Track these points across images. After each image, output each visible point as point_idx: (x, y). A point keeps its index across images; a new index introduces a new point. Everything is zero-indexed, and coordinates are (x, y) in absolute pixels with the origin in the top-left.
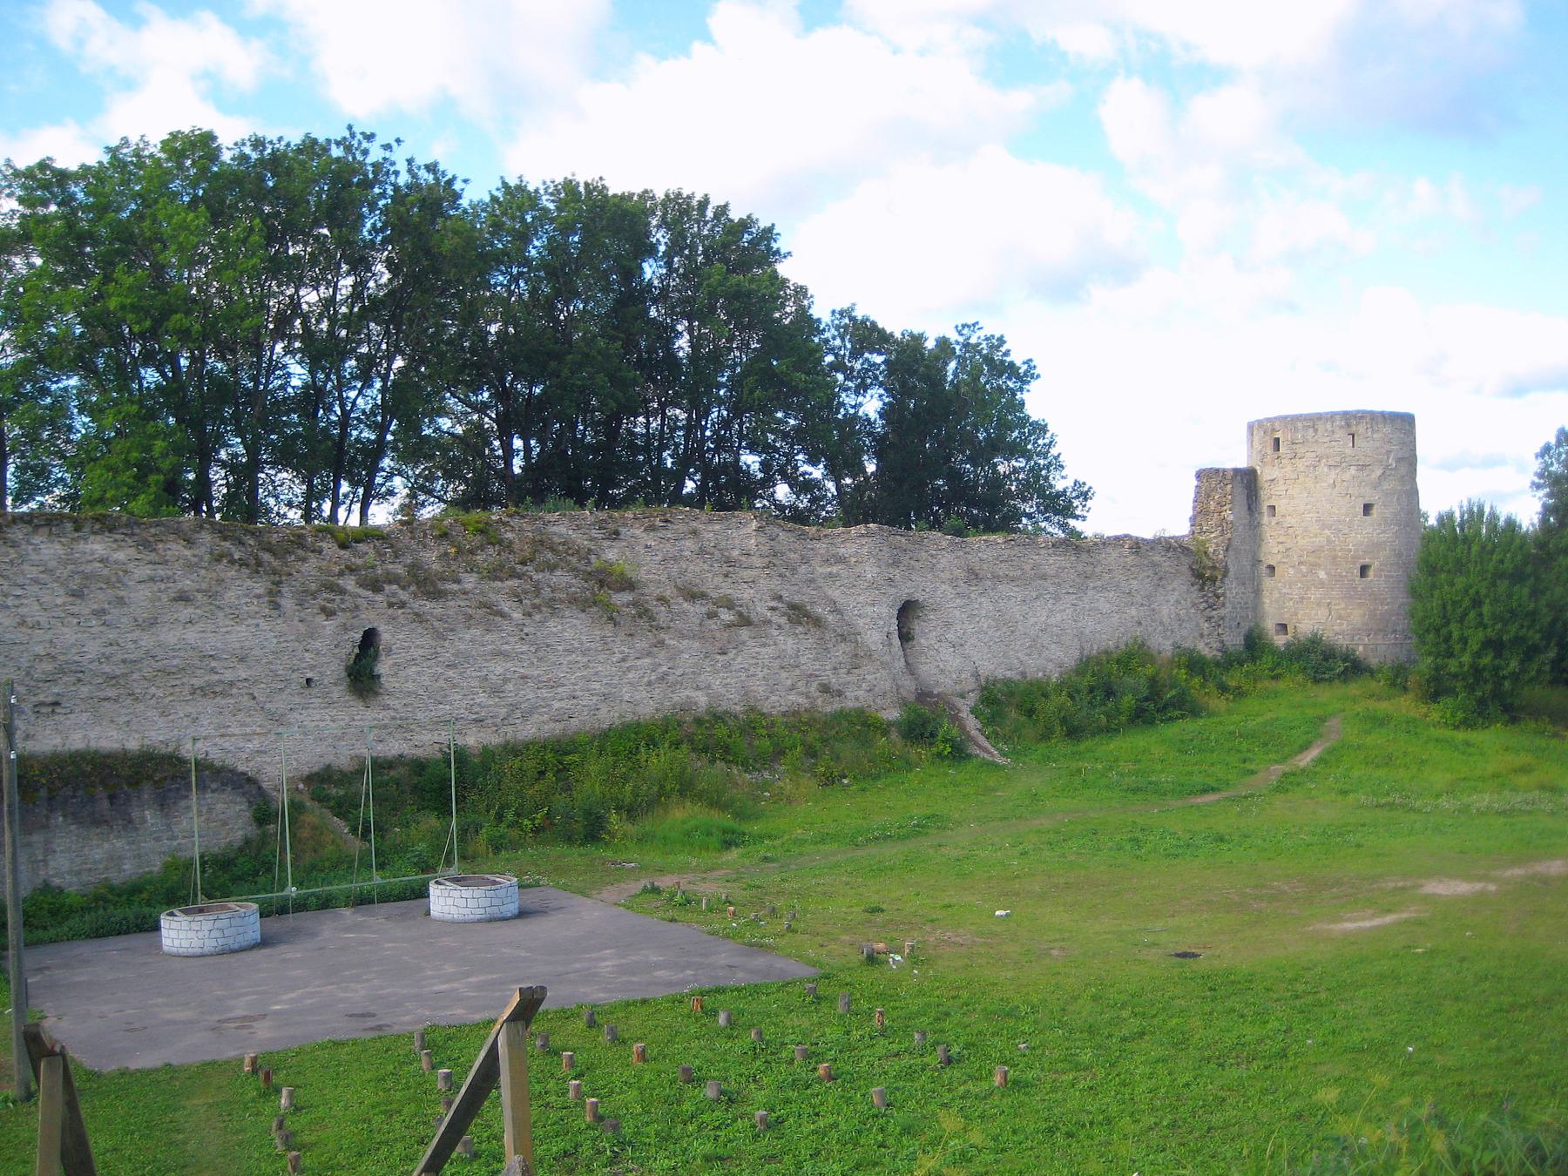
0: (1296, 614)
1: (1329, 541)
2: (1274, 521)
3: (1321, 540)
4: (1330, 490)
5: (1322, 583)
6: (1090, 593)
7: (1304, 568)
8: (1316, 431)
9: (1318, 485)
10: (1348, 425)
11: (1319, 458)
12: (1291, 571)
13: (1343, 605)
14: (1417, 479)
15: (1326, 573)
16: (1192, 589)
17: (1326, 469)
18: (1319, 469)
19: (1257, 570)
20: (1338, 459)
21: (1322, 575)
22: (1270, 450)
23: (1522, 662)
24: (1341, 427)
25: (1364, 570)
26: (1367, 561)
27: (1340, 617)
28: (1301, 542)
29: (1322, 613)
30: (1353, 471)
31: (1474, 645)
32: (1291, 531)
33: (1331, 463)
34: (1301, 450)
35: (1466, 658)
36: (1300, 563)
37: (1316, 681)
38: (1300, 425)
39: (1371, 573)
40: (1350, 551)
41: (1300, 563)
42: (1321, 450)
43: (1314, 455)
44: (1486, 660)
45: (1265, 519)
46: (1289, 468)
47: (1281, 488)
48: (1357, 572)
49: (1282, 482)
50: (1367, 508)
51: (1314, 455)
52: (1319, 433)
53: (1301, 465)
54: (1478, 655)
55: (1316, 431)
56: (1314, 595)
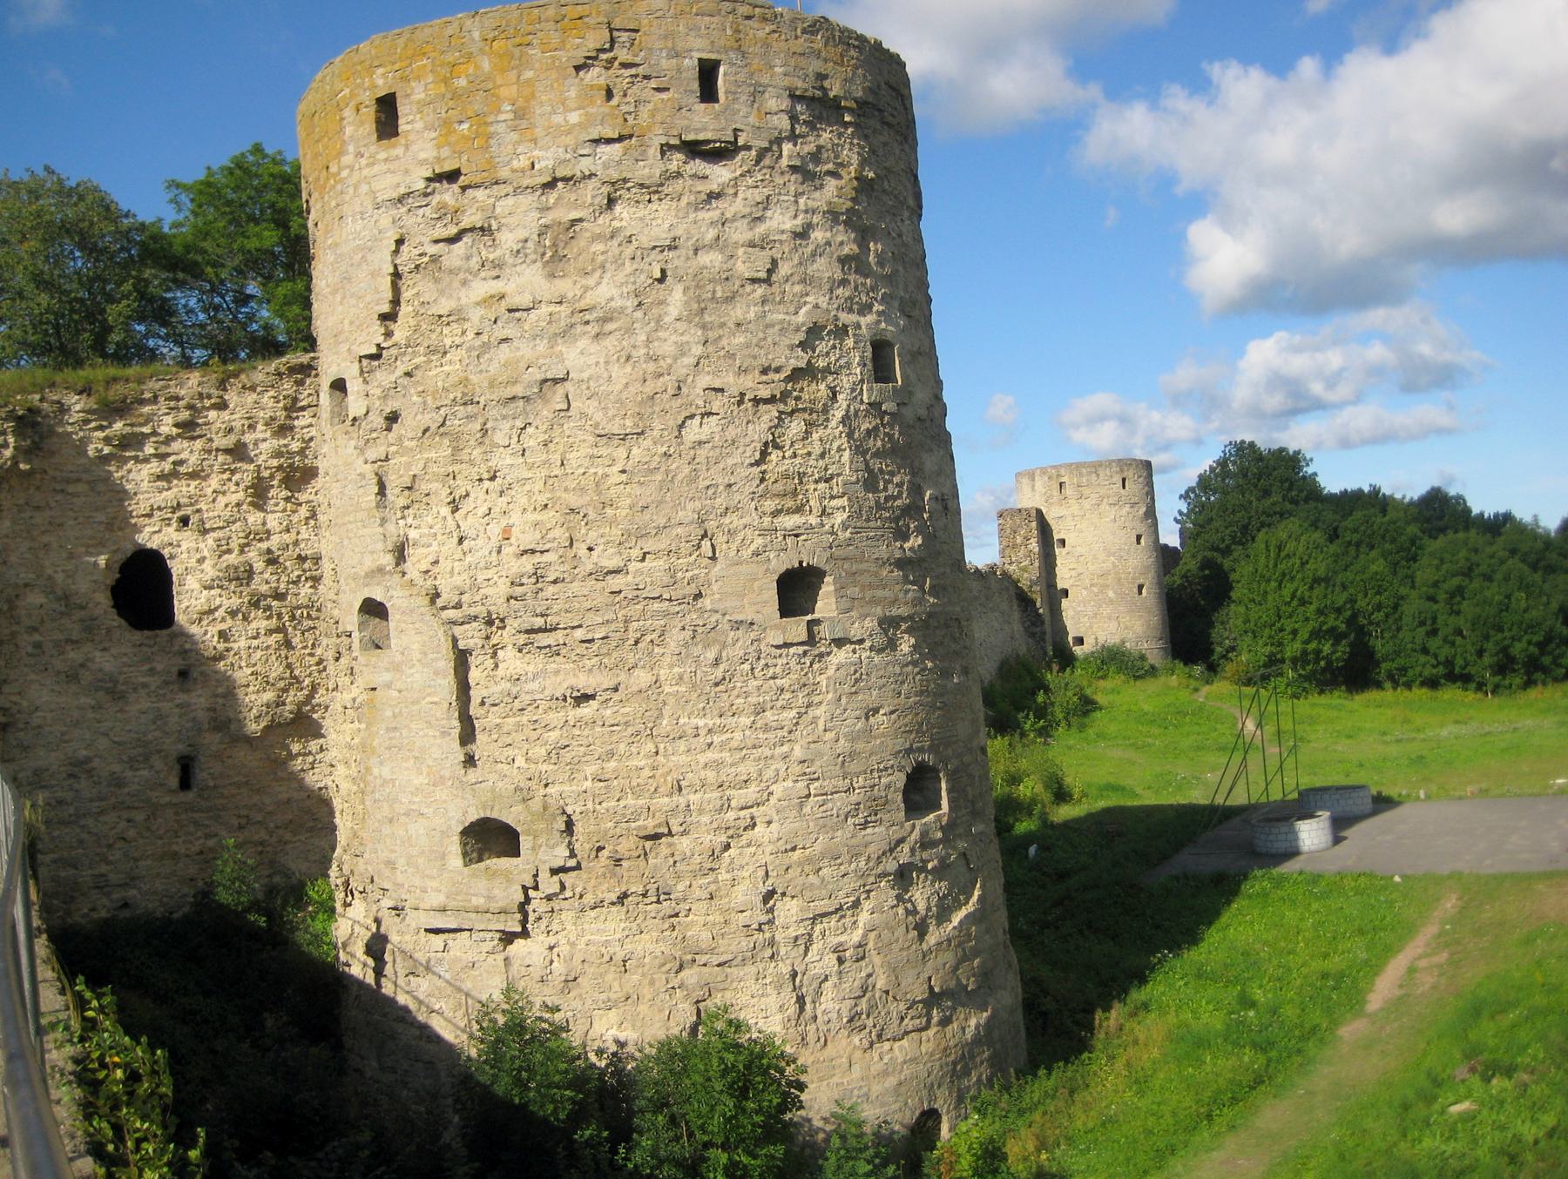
0: (1091, 627)
1: (1115, 566)
2: (1064, 551)
3: (1108, 565)
5: (1111, 601)
7: (1095, 590)
8: (1098, 476)
10: (1122, 471)
11: (1102, 498)
12: (1085, 593)
15: (1115, 593)
19: (1056, 596)
21: (1111, 594)
22: (1056, 492)
23: (1333, 645)
25: (1140, 587)
27: (1126, 628)
28: (1091, 568)
29: (1113, 626)
30: (1127, 508)
31: (1304, 634)
32: (1081, 559)
34: (1086, 491)
35: (1297, 646)
36: (1092, 585)
38: (1084, 471)
39: (1144, 591)
41: (1092, 585)
42: (1103, 491)
44: (1313, 646)
45: (1057, 551)
47: (1069, 523)
48: (1136, 590)
49: (1069, 518)
50: (1139, 538)
53: (1087, 504)
54: (1307, 642)
55: (1098, 476)
56: (1106, 611)
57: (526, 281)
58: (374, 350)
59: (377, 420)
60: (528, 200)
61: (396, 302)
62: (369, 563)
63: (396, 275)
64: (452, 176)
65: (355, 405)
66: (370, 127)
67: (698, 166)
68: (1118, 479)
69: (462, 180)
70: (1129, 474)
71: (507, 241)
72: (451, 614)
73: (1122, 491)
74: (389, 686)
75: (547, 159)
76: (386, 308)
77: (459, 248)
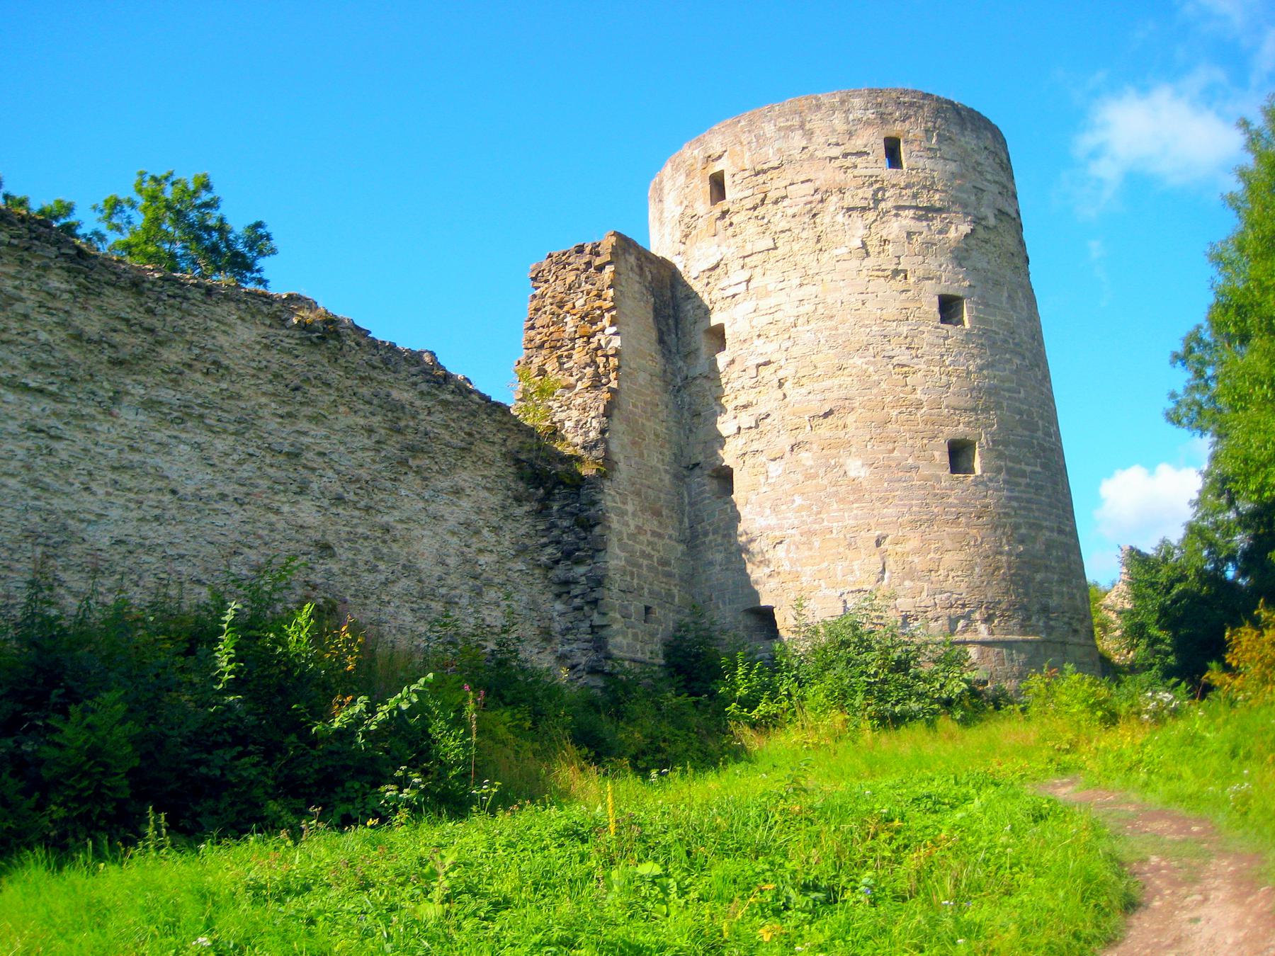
1: (863, 377)
4: (855, 263)
5: (856, 488)
6: (129, 416)
8: (809, 134)
9: (825, 257)
13: (914, 543)
14: (1033, 278)
16: (519, 511)
17: (840, 218)
18: (824, 219)
20: (869, 193)
21: (856, 468)
22: (702, 205)
24: (868, 123)
26: (960, 430)
27: (911, 574)
33: (848, 201)
34: (776, 186)
37: (891, 721)
40: (919, 405)
42: (827, 175)
43: (809, 188)
46: (752, 228)
48: (941, 456)
51: (809, 188)
52: (819, 139)
55: (809, 134)
68: (872, 140)
70: (911, 132)
73: (884, 171)
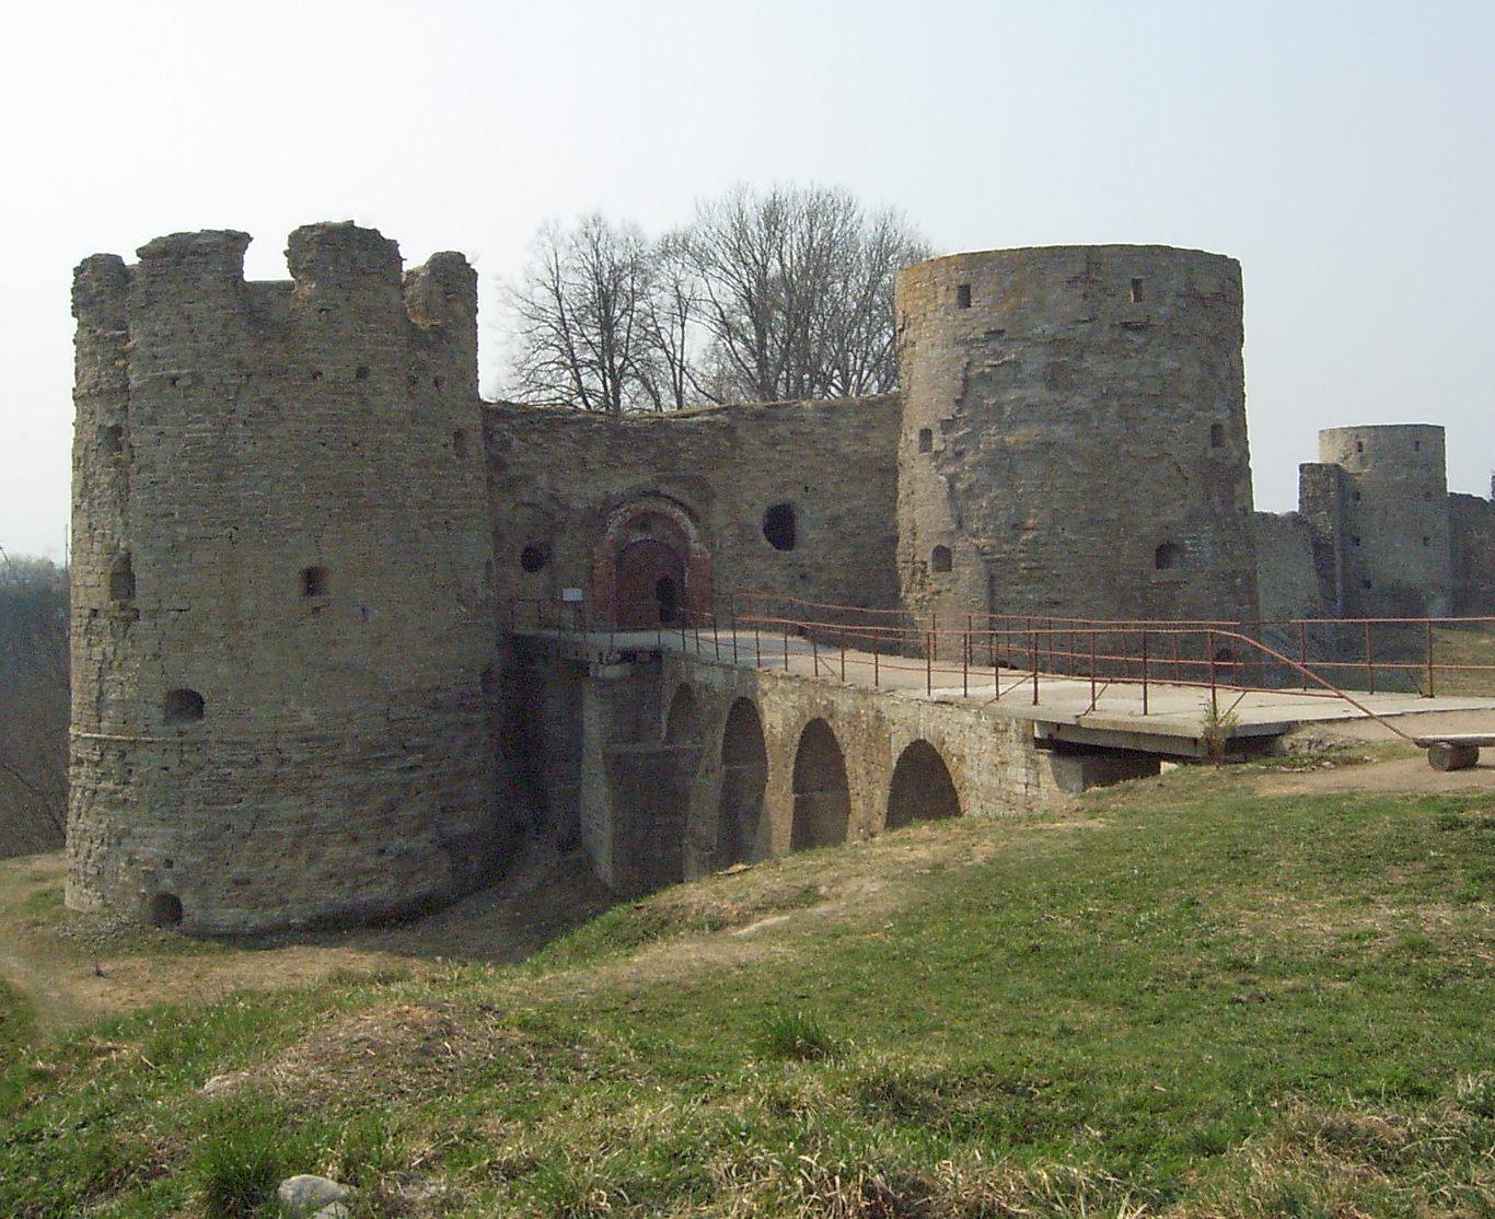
57: (1037, 392)
58: (951, 418)
59: (950, 454)
60: (1040, 350)
61: (964, 394)
62: (941, 527)
63: (966, 380)
64: (1001, 332)
65: (937, 444)
66: (953, 300)
67: (1129, 335)
69: (1006, 336)
71: (1029, 369)
72: (987, 557)
74: (949, 590)
75: (1050, 329)
76: (958, 397)
77: (1002, 371)
